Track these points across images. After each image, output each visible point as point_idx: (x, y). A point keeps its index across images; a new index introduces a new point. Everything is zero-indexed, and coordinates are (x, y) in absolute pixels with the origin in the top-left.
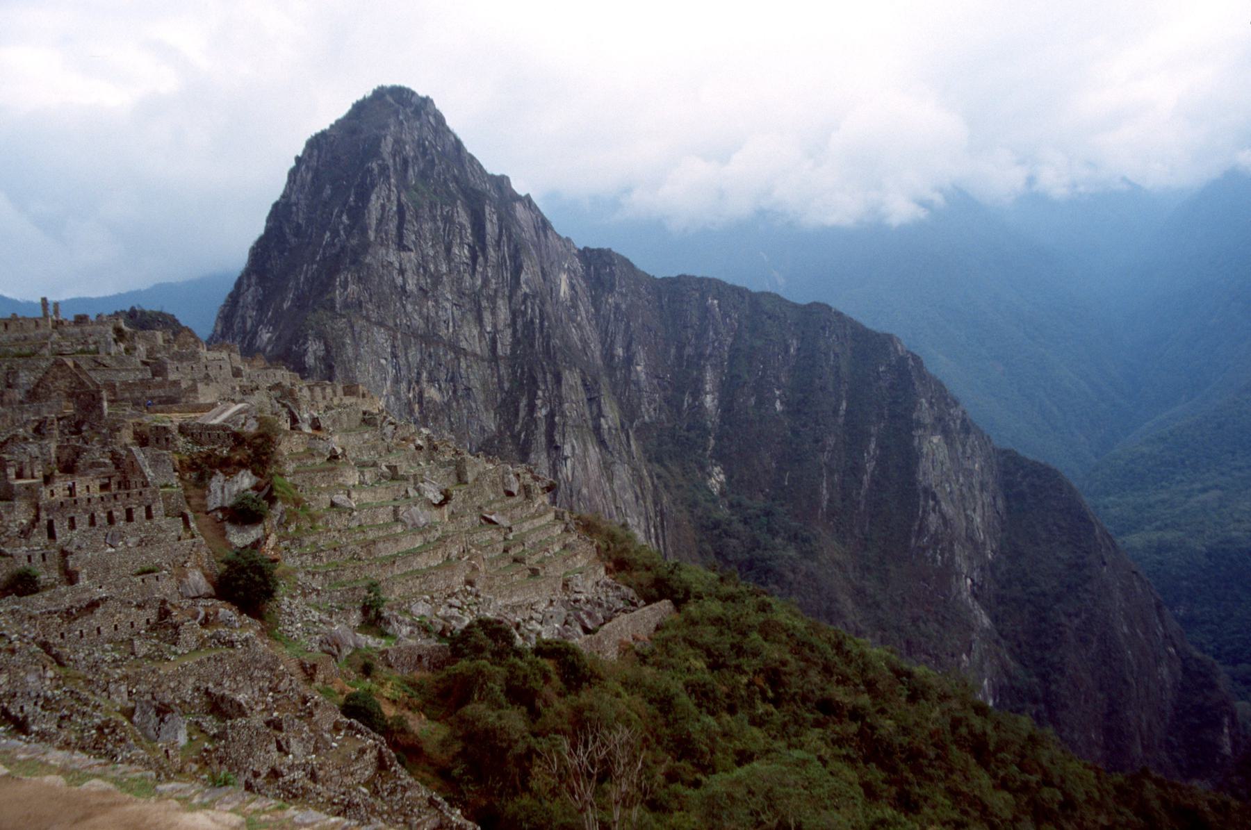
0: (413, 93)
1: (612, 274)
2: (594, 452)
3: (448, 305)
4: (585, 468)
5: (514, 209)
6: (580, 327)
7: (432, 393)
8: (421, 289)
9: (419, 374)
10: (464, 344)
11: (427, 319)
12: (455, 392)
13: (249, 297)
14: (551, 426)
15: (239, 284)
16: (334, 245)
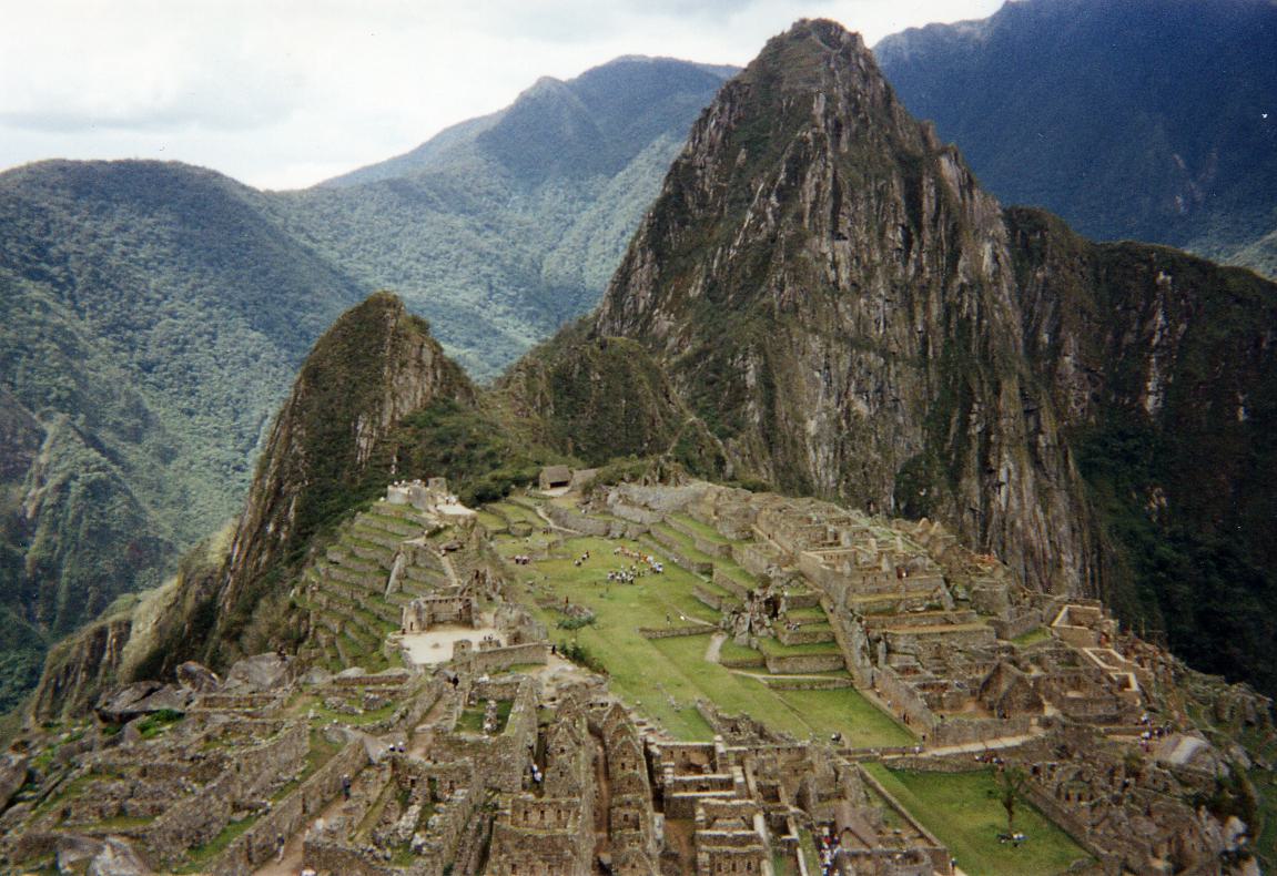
0: (842, 30)
1: (1043, 241)
2: (1029, 473)
3: (880, 301)
4: (1020, 497)
5: (939, 163)
6: (1002, 310)
7: (861, 407)
8: (854, 284)
9: (849, 385)
10: (894, 347)
11: (858, 319)
12: (882, 403)
13: (641, 275)
14: (986, 447)
15: (629, 260)
16: (758, 230)
